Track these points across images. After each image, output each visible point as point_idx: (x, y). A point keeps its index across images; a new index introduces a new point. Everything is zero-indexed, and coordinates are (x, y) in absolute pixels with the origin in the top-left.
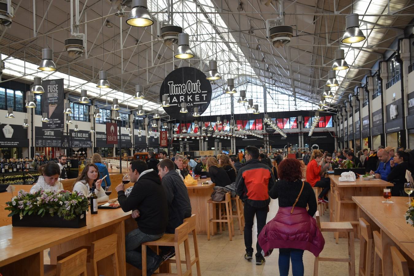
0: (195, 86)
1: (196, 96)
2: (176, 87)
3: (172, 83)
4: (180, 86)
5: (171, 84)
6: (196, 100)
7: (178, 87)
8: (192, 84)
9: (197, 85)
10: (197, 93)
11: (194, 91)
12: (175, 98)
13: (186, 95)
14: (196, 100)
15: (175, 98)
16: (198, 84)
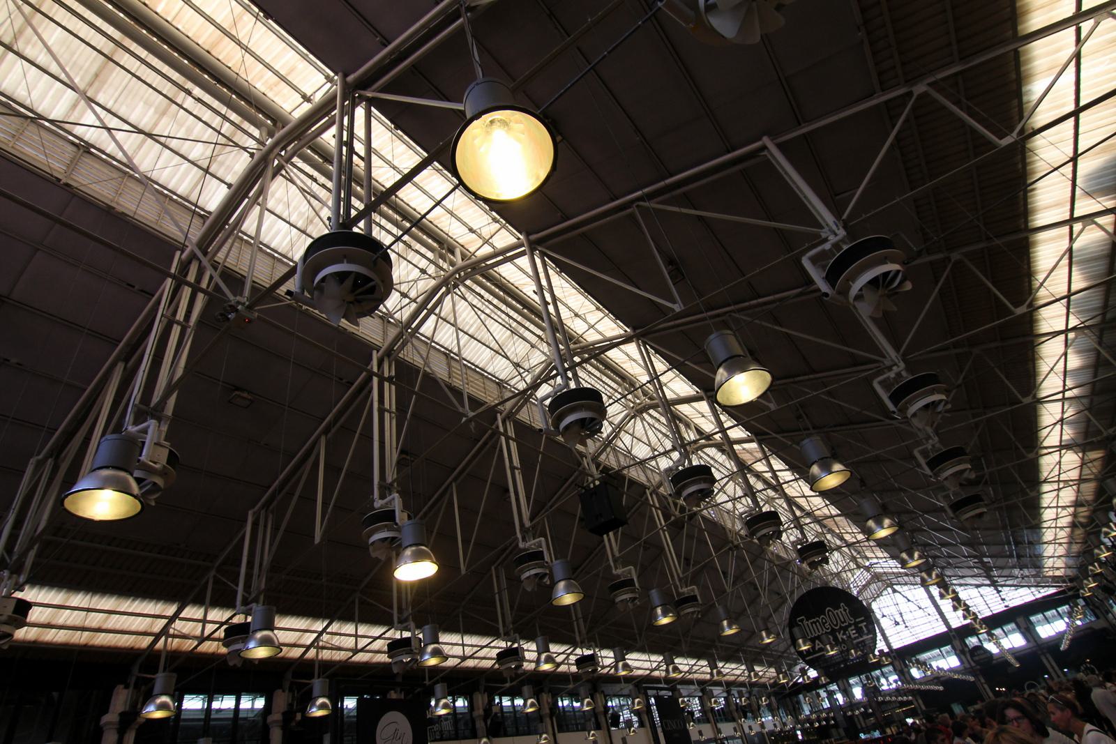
0: (842, 612)
1: (850, 629)
2: (812, 623)
3: (803, 620)
4: (818, 621)
5: (802, 621)
6: (853, 636)
7: (815, 623)
8: (835, 612)
9: (844, 613)
10: (850, 625)
11: (843, 623)
12: (817, 642)
13: (833, 632)
14: (853, 636)
15: (817, 642)
16: (845, 610)
